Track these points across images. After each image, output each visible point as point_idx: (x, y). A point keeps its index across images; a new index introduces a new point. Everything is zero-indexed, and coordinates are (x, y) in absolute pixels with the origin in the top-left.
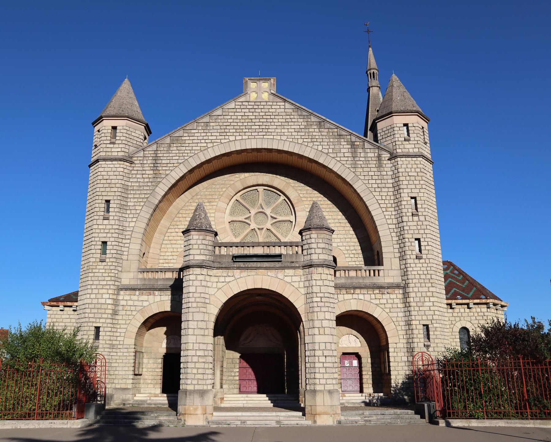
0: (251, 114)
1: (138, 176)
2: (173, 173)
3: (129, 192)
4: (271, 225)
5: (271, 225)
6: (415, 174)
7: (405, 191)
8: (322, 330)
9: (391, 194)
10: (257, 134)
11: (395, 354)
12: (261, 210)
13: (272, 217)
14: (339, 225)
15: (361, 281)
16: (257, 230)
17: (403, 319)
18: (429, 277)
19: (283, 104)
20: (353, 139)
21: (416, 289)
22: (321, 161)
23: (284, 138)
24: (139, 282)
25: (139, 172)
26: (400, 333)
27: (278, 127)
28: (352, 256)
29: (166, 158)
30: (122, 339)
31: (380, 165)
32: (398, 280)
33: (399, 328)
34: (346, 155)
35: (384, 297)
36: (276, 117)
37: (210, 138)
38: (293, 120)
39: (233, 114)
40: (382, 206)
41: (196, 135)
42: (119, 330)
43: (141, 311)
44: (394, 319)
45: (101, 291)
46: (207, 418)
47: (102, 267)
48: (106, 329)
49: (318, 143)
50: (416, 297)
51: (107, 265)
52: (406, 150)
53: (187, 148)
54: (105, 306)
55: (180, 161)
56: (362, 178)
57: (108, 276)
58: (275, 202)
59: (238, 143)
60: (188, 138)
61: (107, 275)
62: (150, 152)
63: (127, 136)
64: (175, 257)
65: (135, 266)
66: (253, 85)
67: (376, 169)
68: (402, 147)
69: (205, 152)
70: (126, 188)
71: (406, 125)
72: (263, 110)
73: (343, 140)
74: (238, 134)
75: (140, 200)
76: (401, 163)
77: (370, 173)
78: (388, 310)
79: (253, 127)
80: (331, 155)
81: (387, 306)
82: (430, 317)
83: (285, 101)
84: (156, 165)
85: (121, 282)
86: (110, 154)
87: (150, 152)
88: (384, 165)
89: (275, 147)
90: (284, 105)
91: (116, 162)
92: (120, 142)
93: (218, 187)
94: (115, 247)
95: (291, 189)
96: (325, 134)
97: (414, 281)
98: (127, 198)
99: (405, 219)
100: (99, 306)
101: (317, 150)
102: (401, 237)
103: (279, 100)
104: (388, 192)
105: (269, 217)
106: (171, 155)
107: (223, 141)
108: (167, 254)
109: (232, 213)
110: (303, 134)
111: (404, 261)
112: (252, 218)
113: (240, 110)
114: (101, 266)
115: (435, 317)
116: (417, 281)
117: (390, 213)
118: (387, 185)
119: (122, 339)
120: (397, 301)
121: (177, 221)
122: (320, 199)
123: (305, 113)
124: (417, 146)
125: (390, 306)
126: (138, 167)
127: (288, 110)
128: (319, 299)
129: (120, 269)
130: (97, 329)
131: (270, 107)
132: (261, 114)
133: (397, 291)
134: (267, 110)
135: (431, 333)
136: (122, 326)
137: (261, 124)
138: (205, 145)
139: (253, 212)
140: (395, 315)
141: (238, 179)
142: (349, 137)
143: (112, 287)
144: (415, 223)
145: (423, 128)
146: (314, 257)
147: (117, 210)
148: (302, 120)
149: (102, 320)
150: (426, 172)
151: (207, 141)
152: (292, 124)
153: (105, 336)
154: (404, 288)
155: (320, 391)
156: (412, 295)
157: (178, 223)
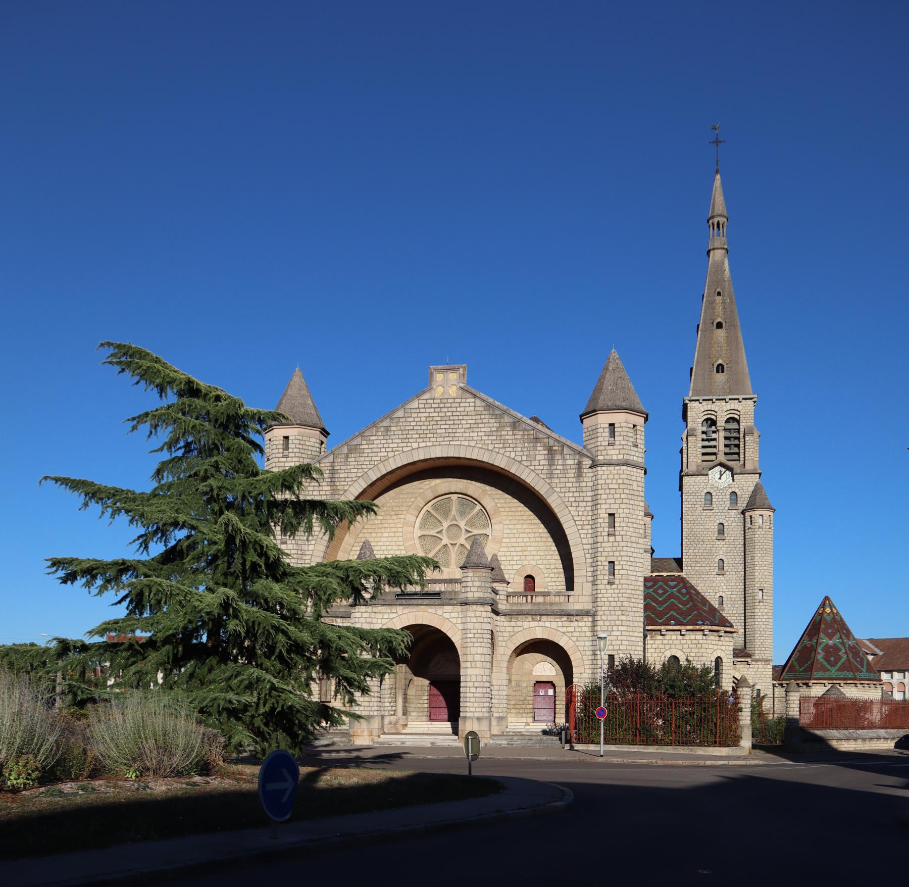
0: (436, 414)
2: (352, 489)
6: (617, 486)
7: (603, 506)
10: (442, 439)
14: (539, 539)
15: (549, 607)
17: (591, 648)
18: (619, 604)
20: (551, 442)
21: (604, 618)
23: (473, 443)
26: (586, 662)
28: (552, 575)
31: (579, 474)
32: (588, 606)
33: (585, 658)
34: (542, 462)
36: (465, 418)
37: (391, 445)
39: (416, 415)
40: (577, 523)
41: (376, 442)
52: (609, 457)
55: (359, 475)
59: (421, 450)
60: (366, 446)
66: (439, 377)
67: (574, 480)
68: (604, 453)
69: (386, 463)
71: (612, 425)
72: (450, 409)
76: (601, 473)
77: (568, 485)
79: (438, 431)
80: (524, 463)
81: (574, 634)
82: (617, 647)
83: (475, 396)
92: (293, 455)
97: (603, 608)
103: (469, 395)
104: (585, 507)
107: (405, 449)
109: (423, 526)
110: (494, 438)
115: (621, 647)
116: (606, 608)
117: (586, 531)
118: (587, 499)
120: (586, 629)
122: (520, 509)
123: (497, 412)
125: (578, 634)
131: (457, 405)
132: (448, 414)
133: (586, 619)
134: (454, 409)
137: (447, 426)
138: (385, 454)
140: (582, 643)
142: (546, 440)
144: (611, 544)
145: (634, 426)
146: (470, 595)
148: (494, 421)
150: (631, 482)
152: (483, 425)
154: (594, 615)
156: (599, 623)
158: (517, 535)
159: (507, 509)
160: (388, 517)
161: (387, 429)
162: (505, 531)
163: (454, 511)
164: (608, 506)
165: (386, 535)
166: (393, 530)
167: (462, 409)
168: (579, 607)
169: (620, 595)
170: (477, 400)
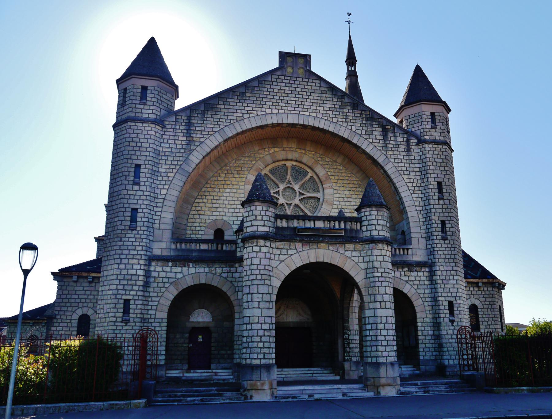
0: (287, 88)
1: (170, 141)
2: (208, 141)
3: (160, 158)
4: (300, 200)
5: (300, 200)
6: (441, 161)
8: (383, 304)
9: (418, 177)
10: (293, 109)
11: (423, 328)
12: (290, 186)
13: (300, 192)
16: (285, 205)
18: (453, 257)
19: (319, 82)
21: (442, 268)
22: (355, 141)
23: (320, 115)
24: (172, 253)
25: (171, 137)
26: (427, 308)
27: (314, 105)
29: (200, 125)
30: (154, 312)
32: (424, 259)
33: (426, 304)
34: (378, 137)
35: (412, 274)
36: (312, 94)
38: (328, 99)
40: (410, 188)
41: (231, 104)
42: (150, 303)
43: (175, 283)
44: (422, 296)
45: (131, 261)
46: (273, 393)
47: (132, 236)
48: (137, 302)
49: (352, 124)
50: (442, 275)
51: (138, 234)
52: (433, 138)
53: (223, 117)
54: (136, 278)
55: (215, 130)
56: (392, 160)
57: (139, 246)
58: (303, 179)
59: (274, 116)
60: (223, 107)
61: (138, 244)
62: (183, 117)
63: (159, 98)
64: (203, 229)
65: (167, 235)
67: (404, 154)
68: (429, 134)
69: (242, 122)
70: (157, 153)
73: (375, 123)
74: (274, 107)
75: (173, 167)
77: (400, 157)
78: (416, 287)
79: (289, 102)
81: (416, 283)
82: (454, 294)
84: (189, 131)
85: (152, 252)
86: (140, 115)
87: (183, 117)
88: (412, 150)
89: (311, 124)
90: (320, 83)
91: (147, 125)
92: (151, 103)
93: (247, 159)
94: (146, 215)
95: (319, 166)
96: (359, 115)
98: (159, 163)
99: (432, 202)
100: (129, 277)
101: (351, 130)
102: (428, 219)
105: (298, 193)
106: (205, 122)
107: (259, 113)
108: (195, 225)
110: (338, 113)
111: (431, 242)
112: (280, 193)
113: (276, 84)
114: (130, 234)
117: (417, 196)
118: (415, 169)
119: (154, 312)
120: (424, 278)
121: (205, 191)
124: (442, 134)
126: (170, 132)
127: (322, 89)
128: (379, 274)
129: (151, 238)
135: (455, 309)
136: (154, 299)
137: (297, 99)
138: (241, 115)
140: (422, 291)
141: (267, 153)
143: (143, 257)
147: (148, 175)
149: (132, 293)
151: (243, 111)
153: (137, 309)
155: (383, 363)
157: (206, 194)
158: (346, 200)
159: (337, 178)
160: (231, 175)
162: (336, 195)
163: (289, 177)
164: (436, 176)
165: (228, 190)
166: (235, 187)
167: (309, 87)
168: (417, 259)
169: (453, 249)
170: (322, 83)
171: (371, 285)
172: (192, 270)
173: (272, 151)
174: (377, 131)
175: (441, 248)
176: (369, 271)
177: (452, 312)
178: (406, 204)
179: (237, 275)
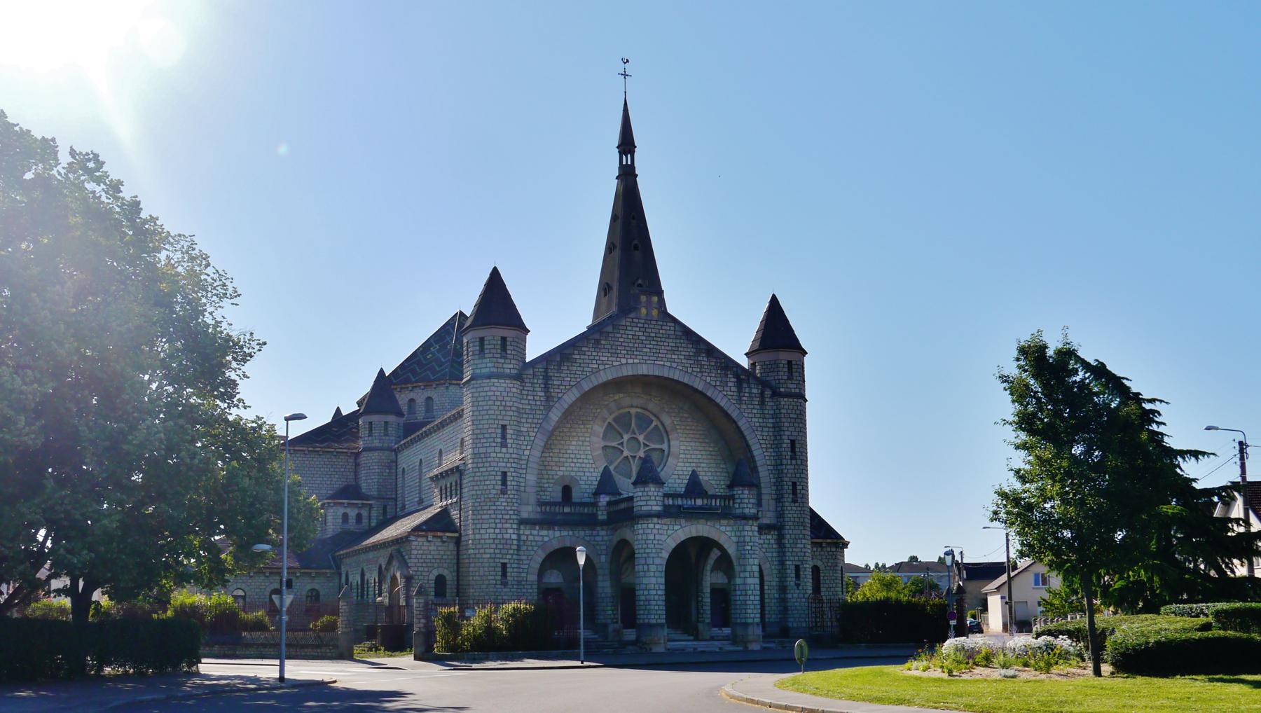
22: (709, 394)
24: (538, 516)
31: (762, 403)
43: (542, 547)
71: (790, 363)
99: (784, 462)
109: (604, 438)
130: (504, 566)
139: (626, 437)
146: (747, 511)
161: (598, 342)
163: (633, 425)
171: (742, 556)
172: (557, 534)
173: (617, 397)
174: (732, 381)
175: (791, 511)
176: (740, 544)
177: (798, 576)
178: (759, 463)
179: (599, 538)
